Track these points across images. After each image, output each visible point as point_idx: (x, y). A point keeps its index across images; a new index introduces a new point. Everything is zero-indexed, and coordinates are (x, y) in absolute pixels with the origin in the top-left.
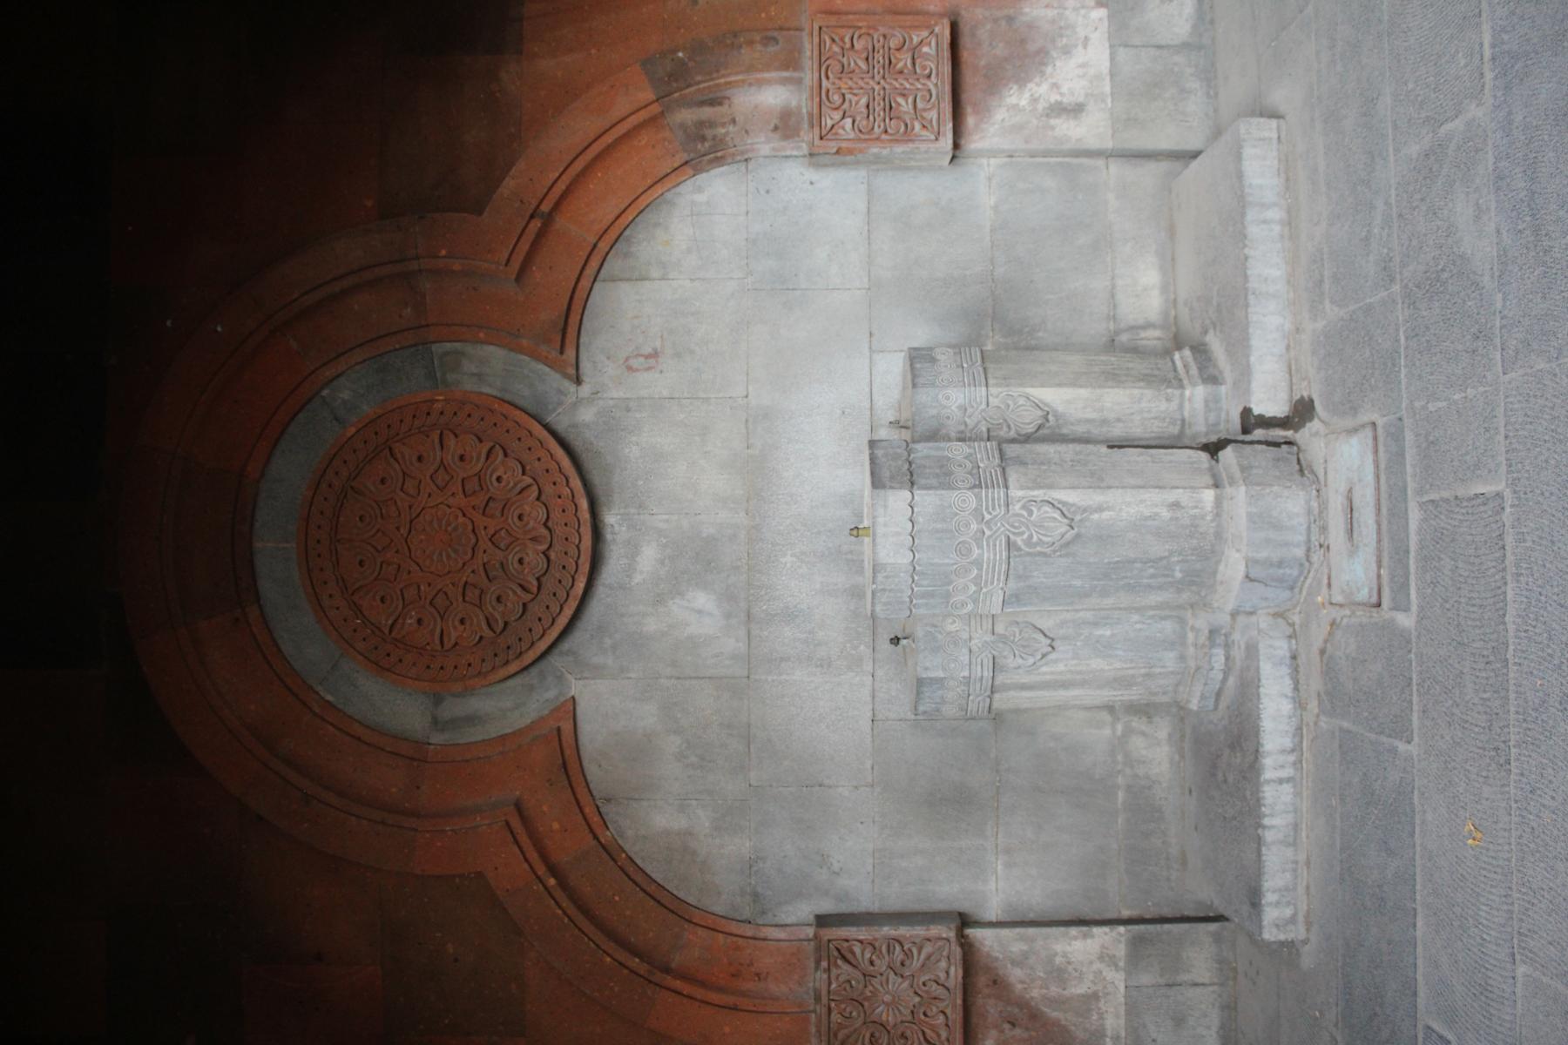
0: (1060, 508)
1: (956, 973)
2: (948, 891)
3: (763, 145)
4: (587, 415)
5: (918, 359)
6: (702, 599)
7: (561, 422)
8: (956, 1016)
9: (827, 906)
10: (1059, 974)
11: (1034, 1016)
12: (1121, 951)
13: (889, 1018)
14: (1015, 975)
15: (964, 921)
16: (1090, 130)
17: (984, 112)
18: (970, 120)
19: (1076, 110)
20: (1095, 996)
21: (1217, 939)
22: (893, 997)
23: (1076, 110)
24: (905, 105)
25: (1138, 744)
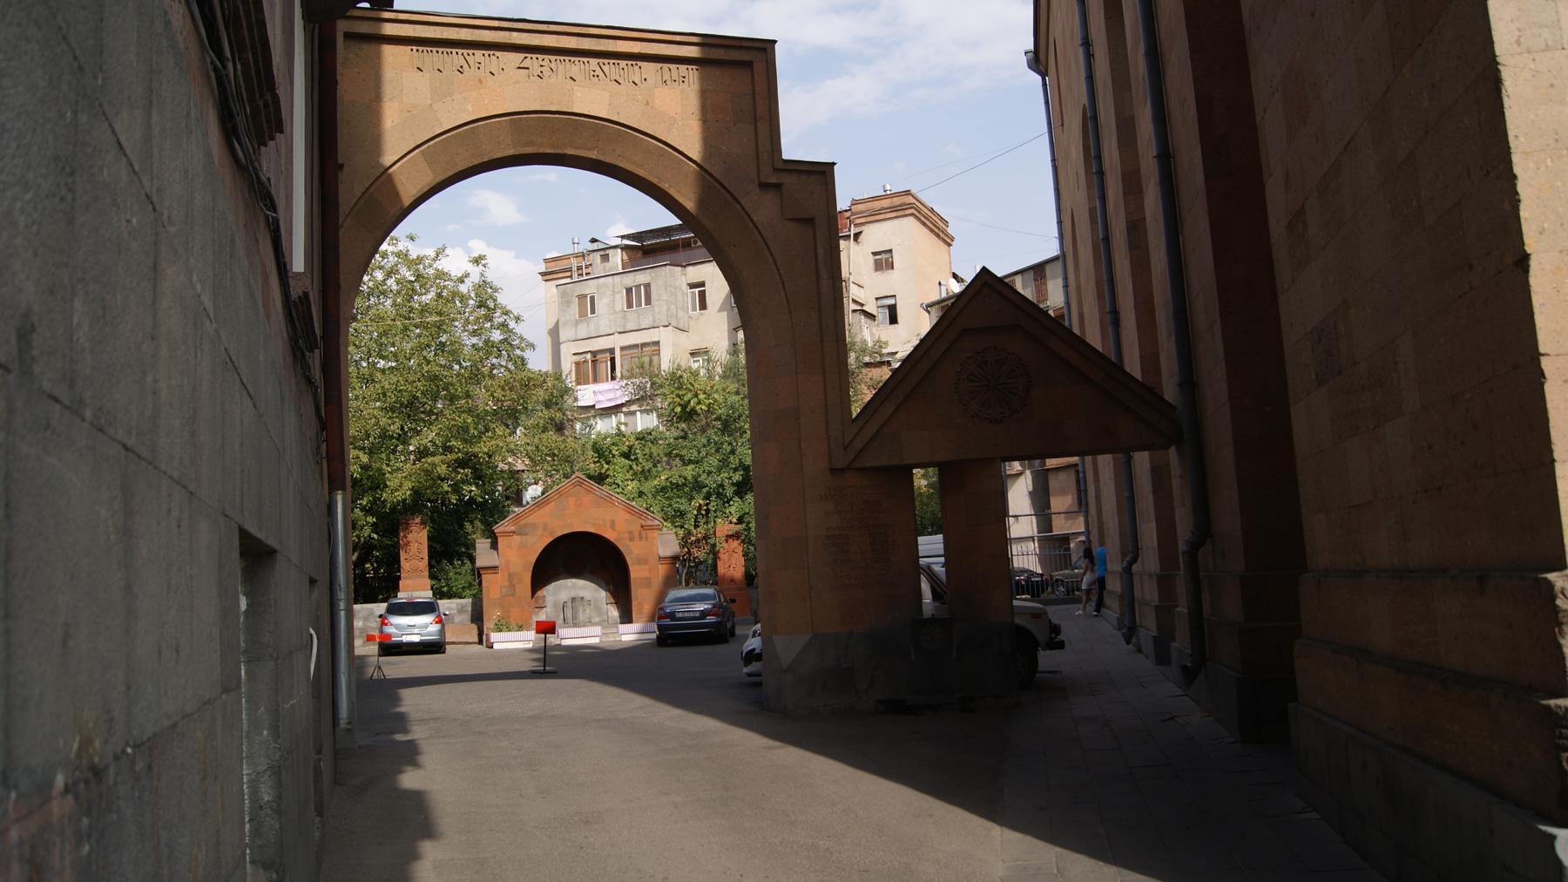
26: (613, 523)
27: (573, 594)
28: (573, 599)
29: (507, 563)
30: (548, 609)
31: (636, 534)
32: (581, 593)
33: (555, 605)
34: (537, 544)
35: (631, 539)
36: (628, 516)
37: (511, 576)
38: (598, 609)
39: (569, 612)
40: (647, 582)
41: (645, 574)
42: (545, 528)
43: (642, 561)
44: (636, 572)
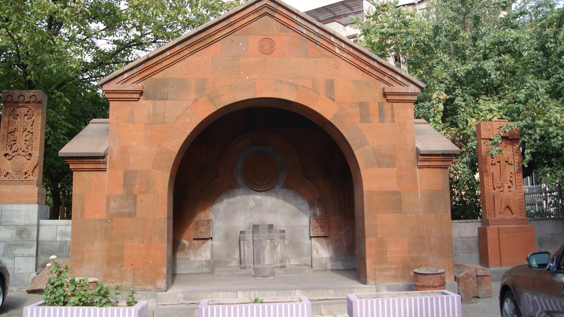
0: (266, 246)
1: (206, 237)
2: (215, 237)
3: (312, 212)
4: (277, 190)
5: (283, 231)
6: (253, 204)
7: (276, 186)
8: (200, 237)
9: (214, 221)
10: (205, 251)
11: (199, 248)
12: (208, 259)
13: (200, 229)
14: (205, 245)
15: (211, 238)
16: (315, 254)
17: (316, 240)
18: (315, 239)
19: (317, 253)
20: (201, 256)
21: (209, 272)
22: (203, 229)
23: (317, 253)
24: (317, 230)
25: (234, 262)
26: (330, 86)
27: (256, 219)
28: (256, 227)
29: (124, 151)
30: (216, 242)
31: (374, 109)
32: (270, 219)
33: (227, 236)
34: (185, 115)
35: (365, 117)
36: (358, 75)
37: (128, 178)
38: (295, 246)
39: (248, 251)
40: (394, 201)
41: (391, 185)
42: (201, 87)
43: (384, 160)
44: (373, 180)
